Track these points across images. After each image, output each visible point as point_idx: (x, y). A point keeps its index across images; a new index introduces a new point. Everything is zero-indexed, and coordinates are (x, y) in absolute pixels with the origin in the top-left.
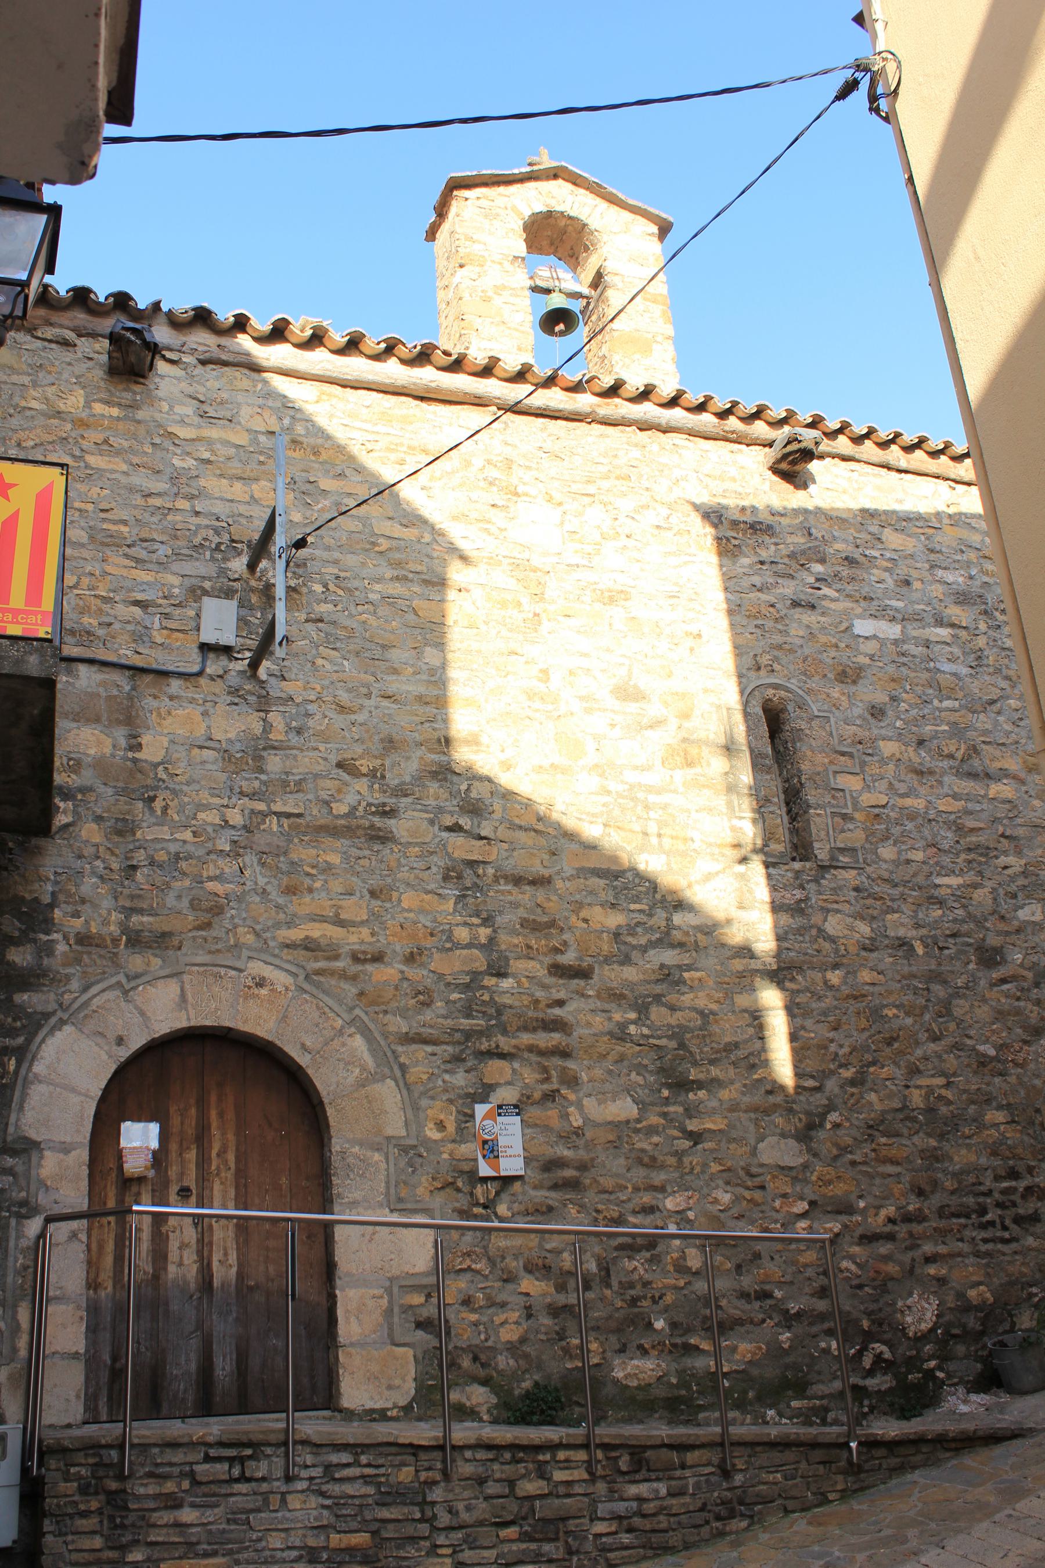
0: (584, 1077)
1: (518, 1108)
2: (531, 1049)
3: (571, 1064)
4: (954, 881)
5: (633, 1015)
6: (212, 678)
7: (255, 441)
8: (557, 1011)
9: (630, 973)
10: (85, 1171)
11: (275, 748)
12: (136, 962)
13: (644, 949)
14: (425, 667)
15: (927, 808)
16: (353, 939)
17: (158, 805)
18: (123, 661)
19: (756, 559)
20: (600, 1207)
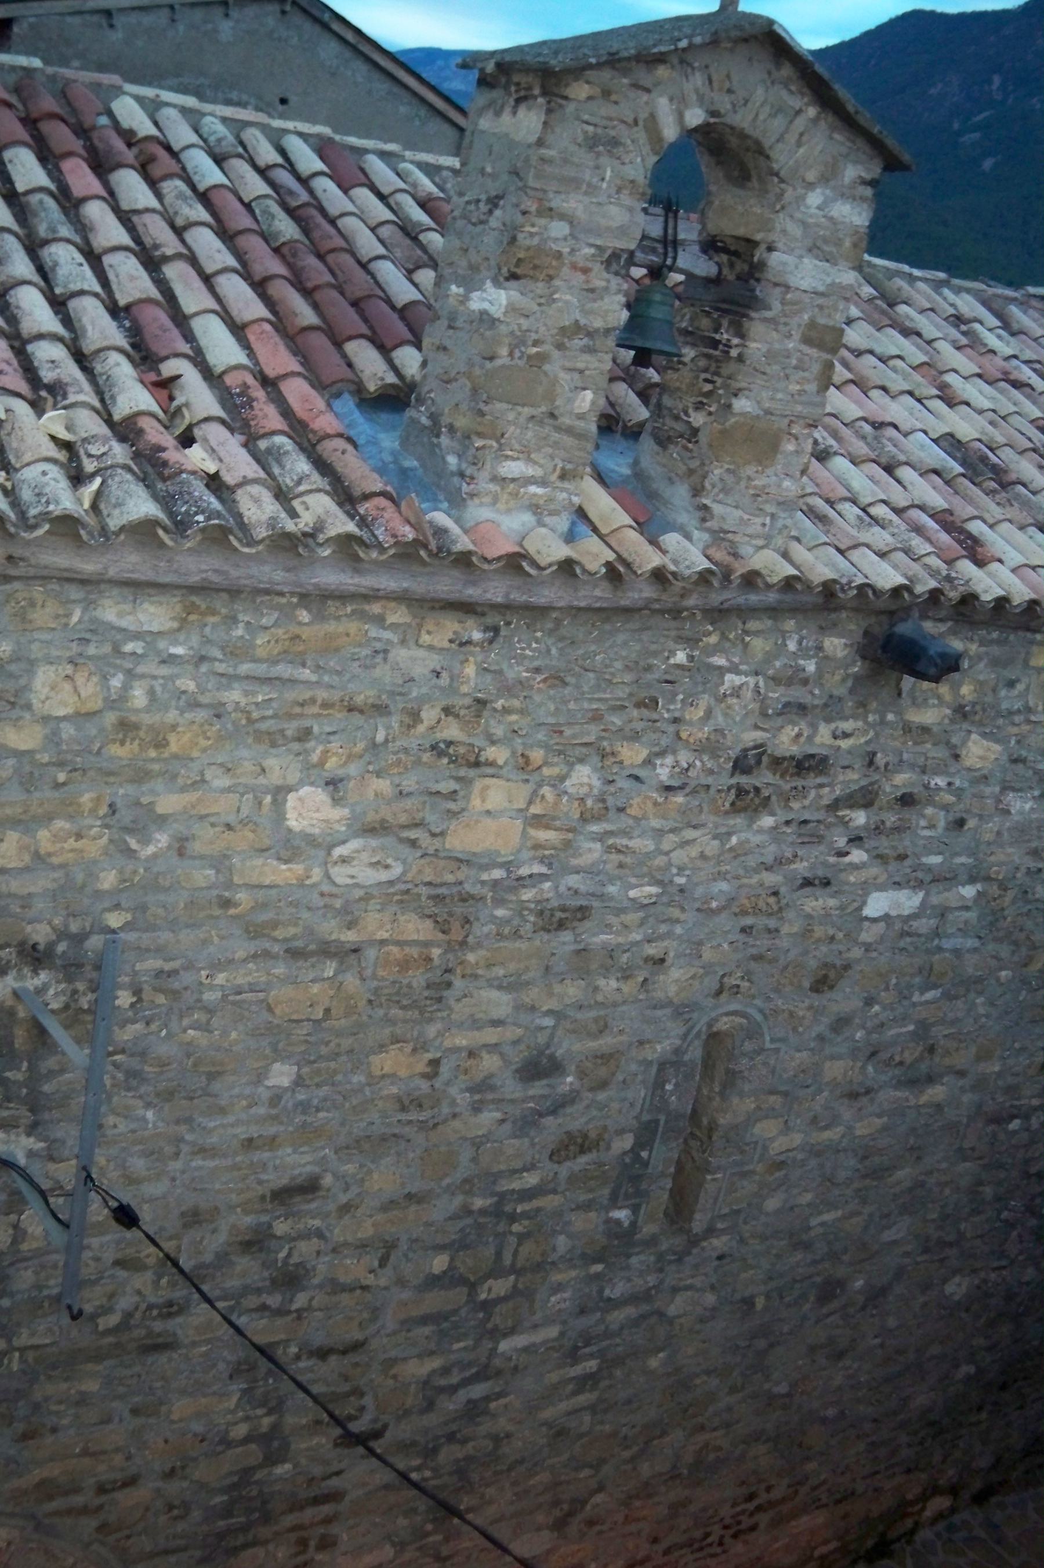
0: (345, 1537)
3: (335, 1529)
7: (53, 739)
8: (334, 1482)
11: (26, 1259)
13: (453, 1389)
14: (264, 1094)
16: (102, 1468)
19: (782, 816)
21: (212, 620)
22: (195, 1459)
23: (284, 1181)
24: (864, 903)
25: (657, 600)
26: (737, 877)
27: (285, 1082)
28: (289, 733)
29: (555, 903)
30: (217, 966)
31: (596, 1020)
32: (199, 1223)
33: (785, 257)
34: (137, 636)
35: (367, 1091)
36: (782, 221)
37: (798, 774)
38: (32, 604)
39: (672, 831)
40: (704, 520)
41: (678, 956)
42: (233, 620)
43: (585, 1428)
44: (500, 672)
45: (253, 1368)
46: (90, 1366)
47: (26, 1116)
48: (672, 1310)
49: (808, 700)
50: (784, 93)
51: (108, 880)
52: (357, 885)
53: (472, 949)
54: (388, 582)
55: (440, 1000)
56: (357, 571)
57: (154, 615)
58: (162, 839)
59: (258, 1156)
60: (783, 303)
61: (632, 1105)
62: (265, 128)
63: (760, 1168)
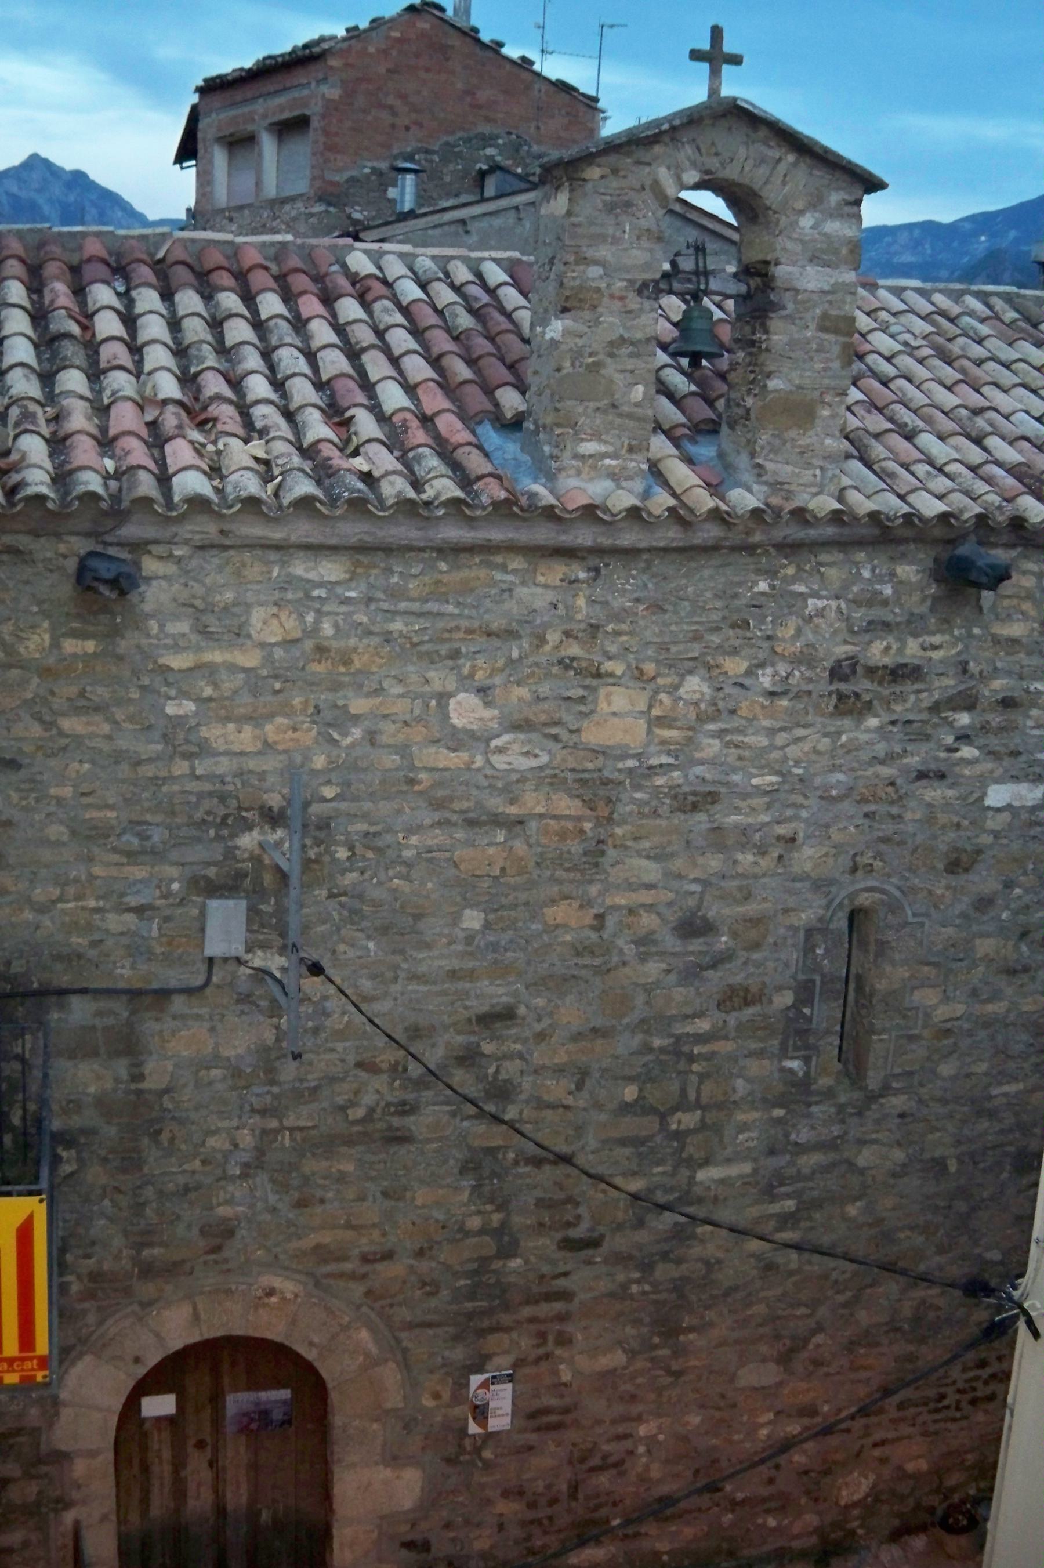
0: (580, 1337)
1: (510, 1378)
2: (532, 1320)
3: (569, 1328)
4: (1012, 1088)
5: (637, 1275)
6: (218, 987)
7: (268, 659)
8: (562, 1282)
9: (642, 1237)
10: (111, 1469)
12: (147, 1289)
14: (461, 935)
15: (1008, 1011)
17: (165, 1137)
18: (121, 985)
19: (886, 718)
21: (374, 571)
22: (439, 1243)
23: (485, 1009)
24: (985, 794)
25: (726, 539)
26: (852, 770)
27: (477, 925)
28: (443, 653)
29: (686, 789)
30: (410, 831)
31: (740, 888)
32: (420, 1037)
33: (790, 269)
34: (321, 585)
35: (545, 938)
36: (781, 242)
37: (894, 681)
38: (244, 565)
39: (783, 729)
40: (759, 475)
41: (808, 837)
42: (392, 572)
43: (793, 1266)
44: (607, 603)
45: (478, 1168)
46: (343, 1149)
47: (279, 942)
48: (861, 1162)
49: (890, 618)
50: (764, 149)
51: (319, 762)
52: (513, 770)
53: (619, 825)
54: (496, 534)
55: (596, 865)
56: (472, 528)
57: (331, 570)
58: (357, 733)
59: (461, 985)
60: (796, 302)
61: (787, 965)
62: (465, 260)
63: (926, 1033)
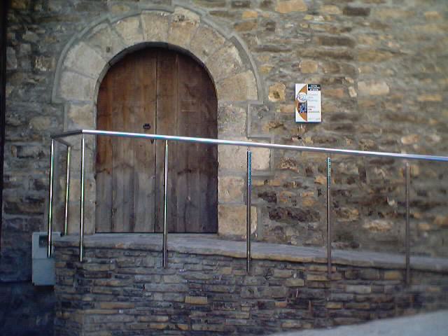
3: (352, 64)
8: (346, 35)
20: (363, 140)
